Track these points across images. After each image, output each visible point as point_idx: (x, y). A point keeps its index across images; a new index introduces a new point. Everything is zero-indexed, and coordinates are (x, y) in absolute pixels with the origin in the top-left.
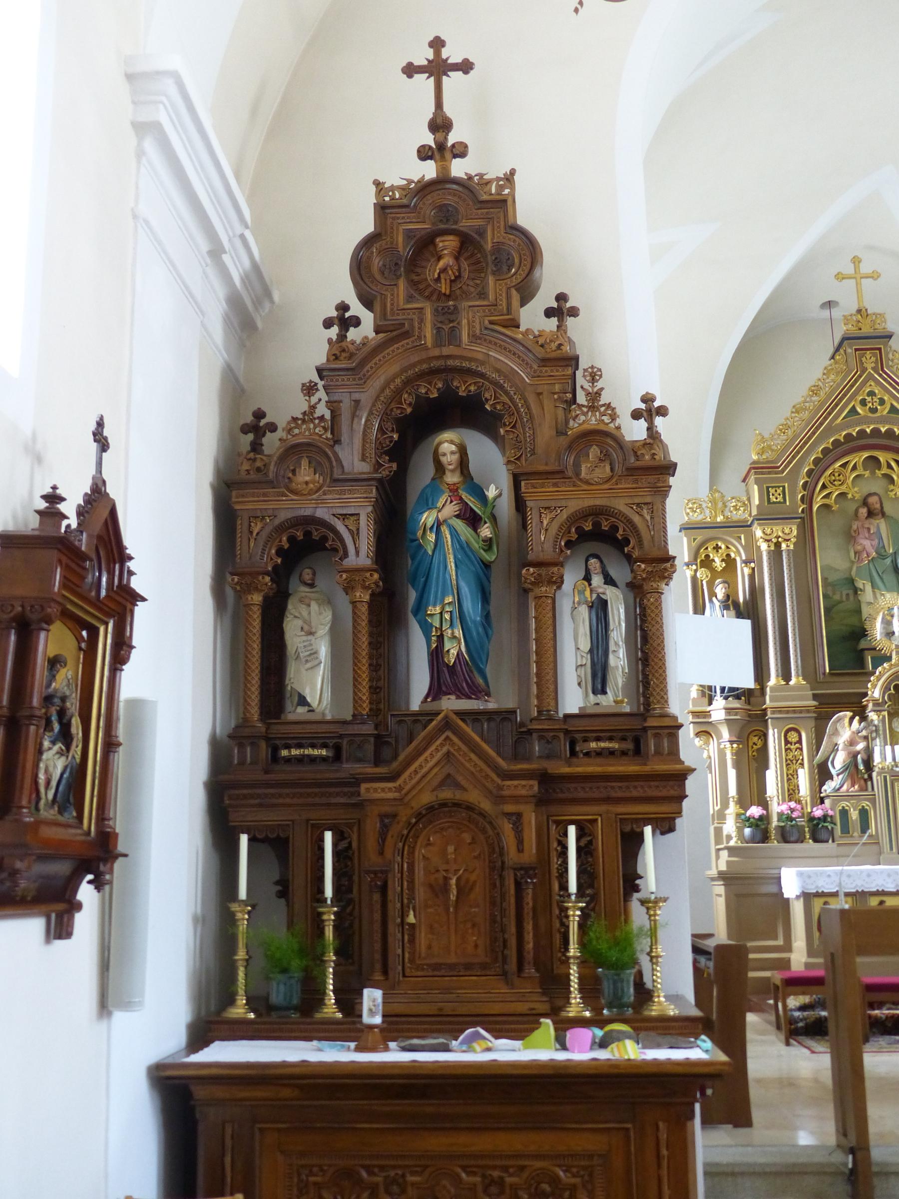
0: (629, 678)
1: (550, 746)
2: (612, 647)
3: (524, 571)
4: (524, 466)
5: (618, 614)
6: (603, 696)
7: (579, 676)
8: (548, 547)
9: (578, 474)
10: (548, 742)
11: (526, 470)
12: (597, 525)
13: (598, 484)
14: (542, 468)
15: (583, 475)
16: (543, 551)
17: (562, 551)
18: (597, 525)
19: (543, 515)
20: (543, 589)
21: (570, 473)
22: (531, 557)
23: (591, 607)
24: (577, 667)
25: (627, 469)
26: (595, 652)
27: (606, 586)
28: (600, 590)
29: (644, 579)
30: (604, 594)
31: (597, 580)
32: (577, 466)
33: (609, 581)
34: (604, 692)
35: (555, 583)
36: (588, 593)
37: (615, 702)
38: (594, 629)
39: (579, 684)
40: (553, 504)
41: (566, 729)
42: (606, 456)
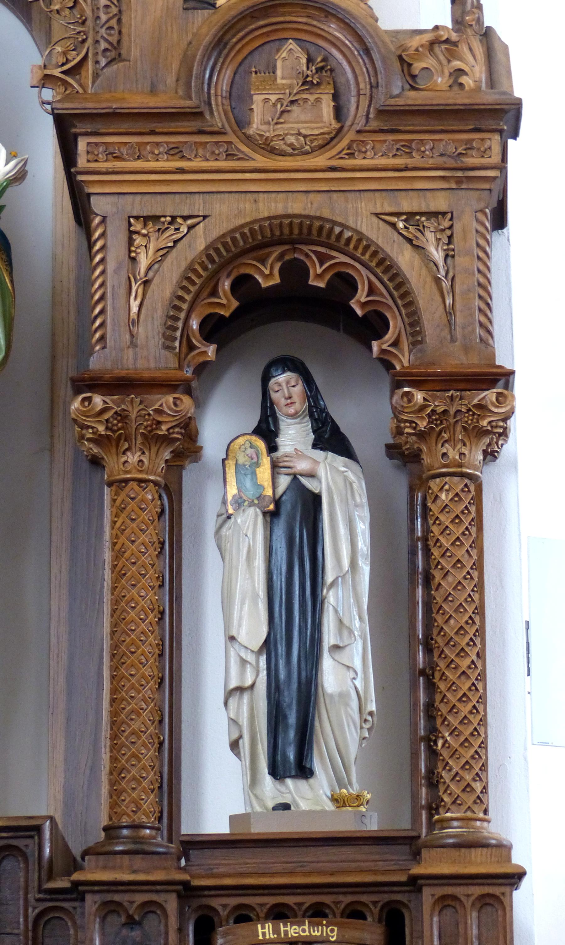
0: (377, 728)
1: (136, 934)
2: (329, 637)
3: (76, 404)
4: (94, 92)
5: (350, 539)
6: (302, 784)
7: (234, 722)
8: (150, 331)
9: (241, 123)
10: (131, 923)
11: (90, 106)
12: (294, 271)
13: (297, 152)
14: (138, 101)
15: (256, 126)
16: (133, 345)
17: (191, 347)
18: (294, 271)
19: (138, 240)
20: (133, 458)
21: (218, 119)
22: (98, 362)
23: (272, 516)
24: (230, 694)
25: (382, 113)
26: (281, 649)
27: (319, 454)
28: (302, 466)
29: (422, 435)
30: (311, 475)
31: (294, 435)
32: (239, 98)
33: (330, 438)
34: (304, 771)
35: (166, 440)
36: (264, 473)
37: (334, 799)
38: (280, 582)
39: (235, 746)
40: (168, 207)
41: (186, 884)
42: (320, 73)
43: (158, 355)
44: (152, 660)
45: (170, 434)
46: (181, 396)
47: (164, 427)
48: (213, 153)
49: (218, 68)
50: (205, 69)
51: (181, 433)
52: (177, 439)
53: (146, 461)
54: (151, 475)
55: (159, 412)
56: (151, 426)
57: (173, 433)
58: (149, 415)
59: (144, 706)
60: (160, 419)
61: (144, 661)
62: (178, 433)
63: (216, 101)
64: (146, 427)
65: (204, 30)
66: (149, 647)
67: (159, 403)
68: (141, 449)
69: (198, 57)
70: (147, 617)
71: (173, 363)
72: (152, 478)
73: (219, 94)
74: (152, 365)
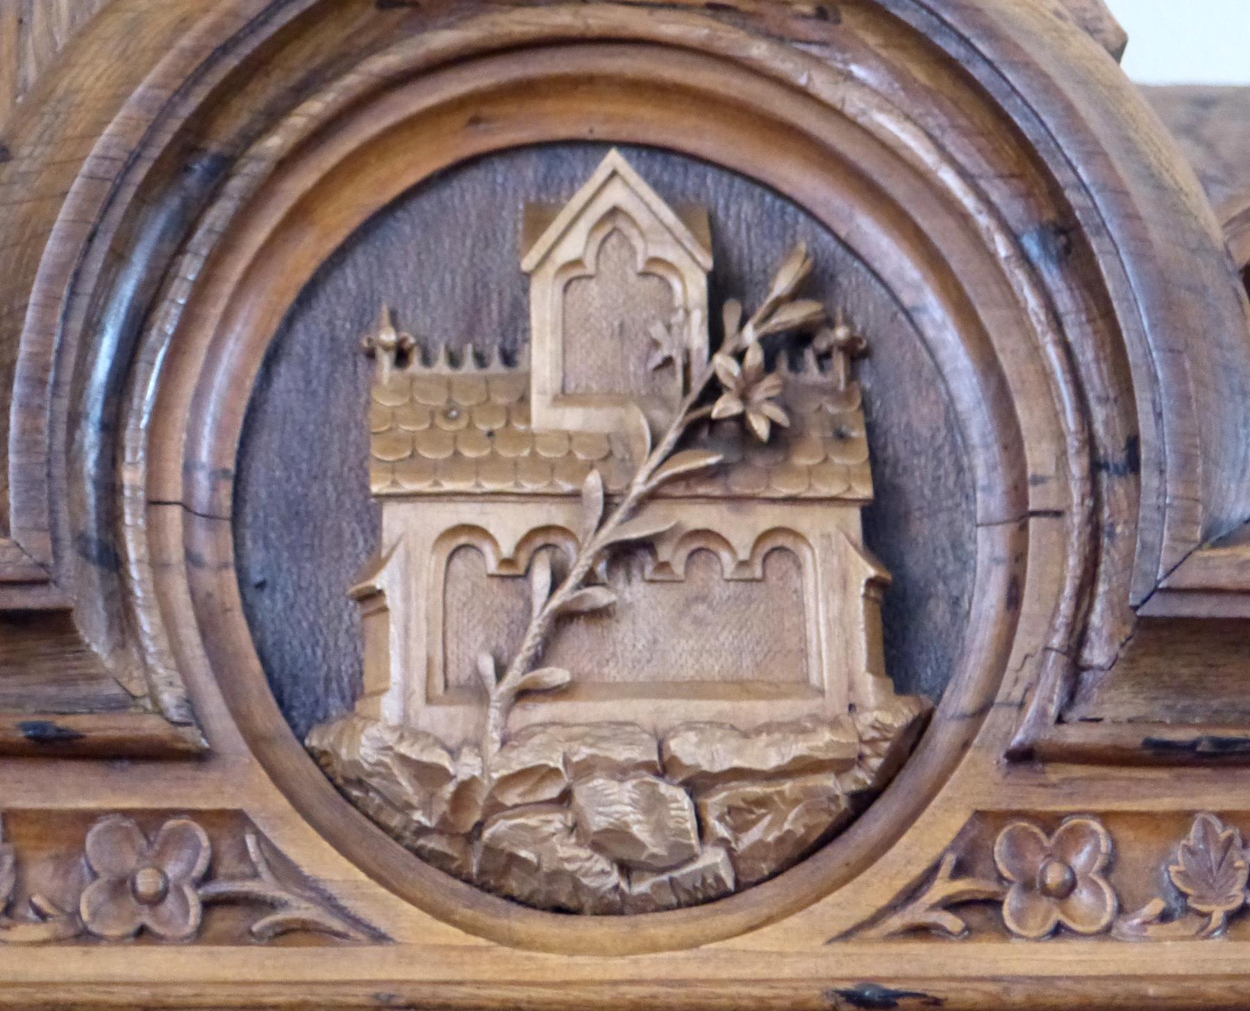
9: (305, 689)
15: (399, 713)
42: (786, 371)
48: (122, 886)
49: (167, 322)
50: (93, 328)
63: (153, 530)
65: (93, 73)
69: (52, 248)
73: (173, 489)
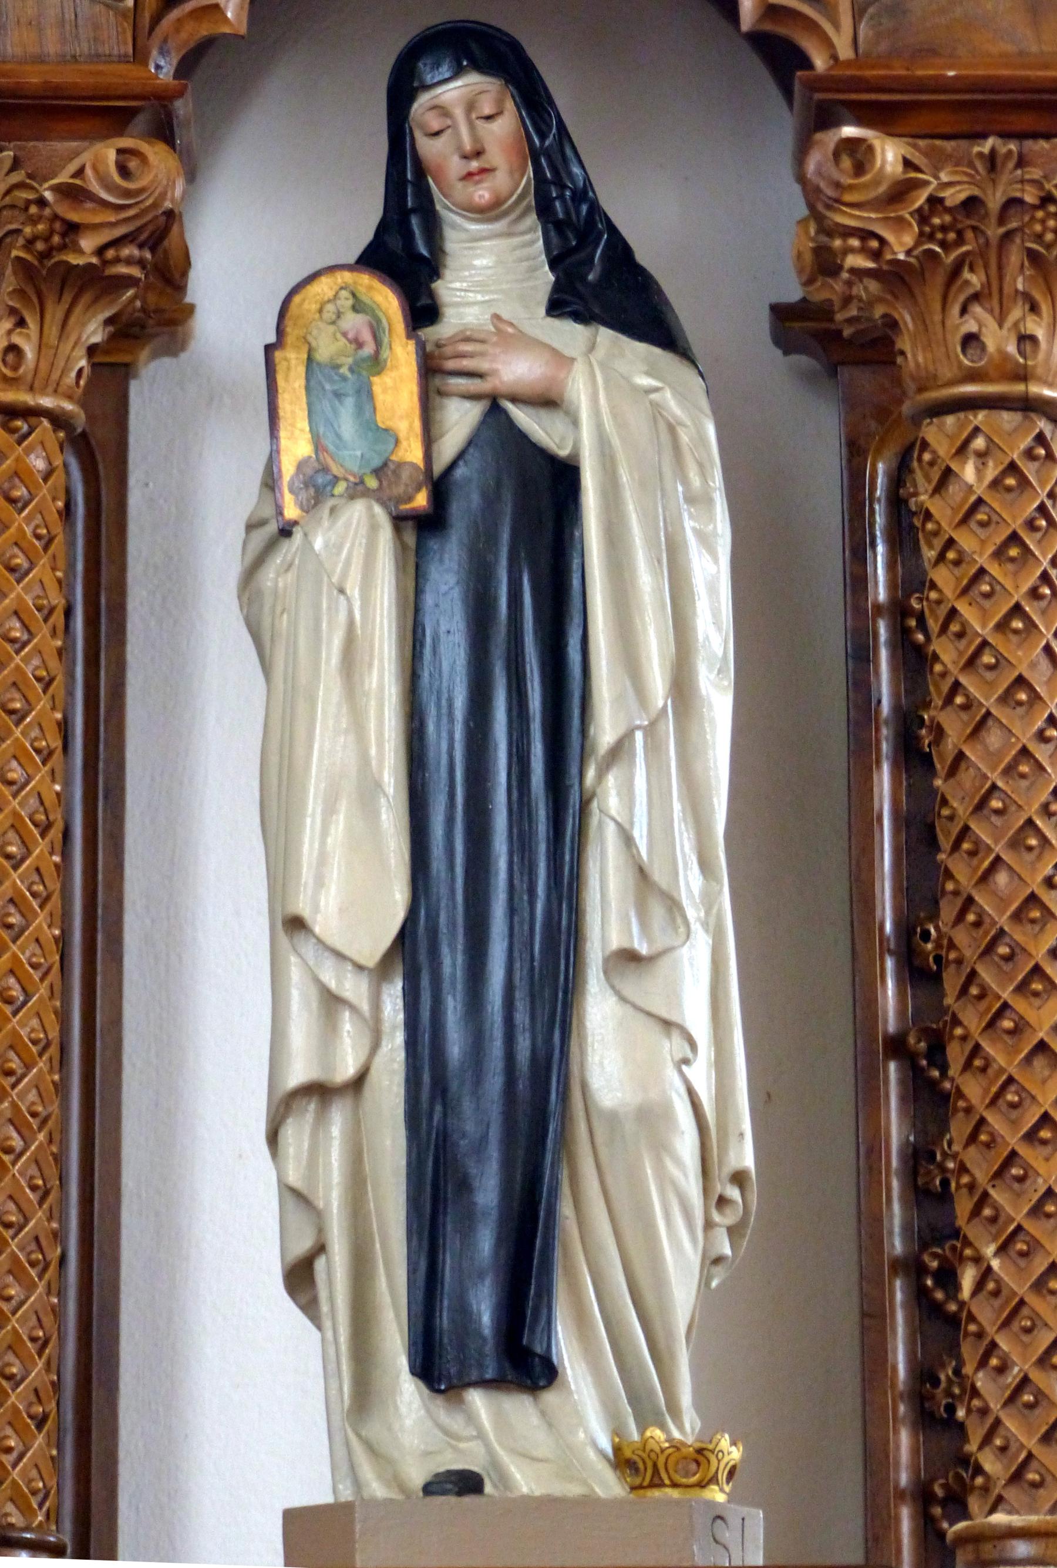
2: (608, 919)
5: (672, 602)
23: (421, 529)
26: (452, 961)
27: (569, 335)
28: (516, 370)
30: (547, 401)
31: (492, 273)
33: (602, 282)
35: (95, 282)
36: (398, 390)
38: (448, 740)
43: (69, 16)
44: (43, 990)
45: (106, 263)
46: (144, 147)
47: (88, 243)
51: (141, 263)
52: (129, 281)
53: (30, 353)
54: (43, 392)
55: (73, 193)
56: (47, 239)
57: (117, 260)
58: (42, 202)
59: (17, 1142)
60: (74, 217)
61: (16, 992)
62: (129, 261)
64: (30, 243)
66: (33, 947)
67: (72, 167)
68: (13, 311)
70: (29, 852)
71: (117, 41)
72: (47, 402)
74: (52, 47)
